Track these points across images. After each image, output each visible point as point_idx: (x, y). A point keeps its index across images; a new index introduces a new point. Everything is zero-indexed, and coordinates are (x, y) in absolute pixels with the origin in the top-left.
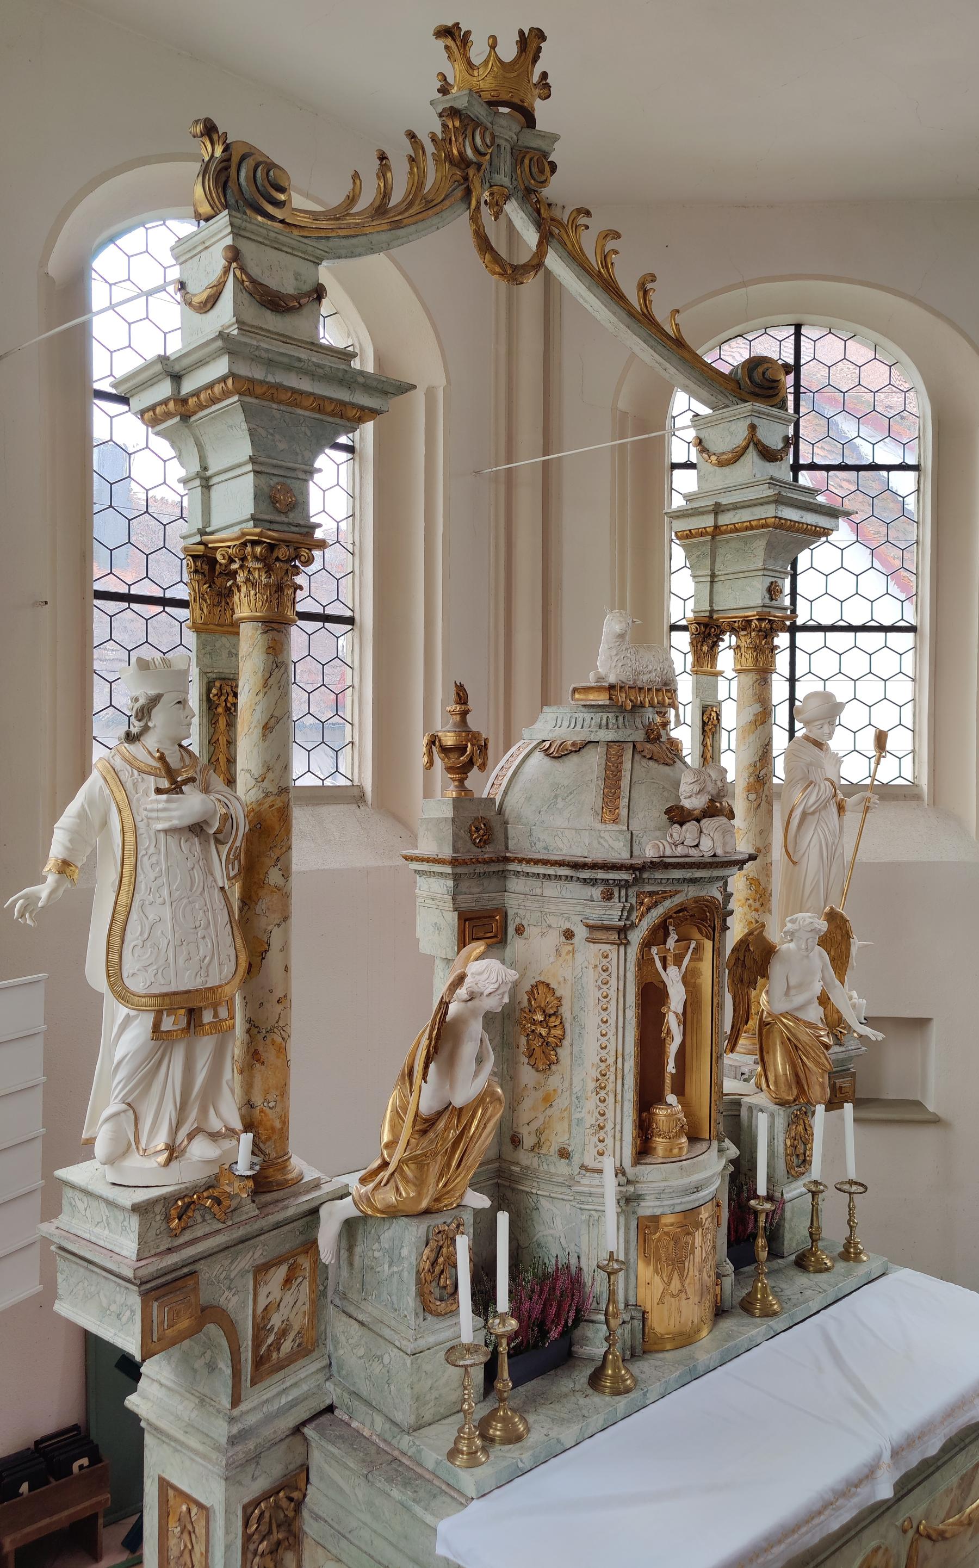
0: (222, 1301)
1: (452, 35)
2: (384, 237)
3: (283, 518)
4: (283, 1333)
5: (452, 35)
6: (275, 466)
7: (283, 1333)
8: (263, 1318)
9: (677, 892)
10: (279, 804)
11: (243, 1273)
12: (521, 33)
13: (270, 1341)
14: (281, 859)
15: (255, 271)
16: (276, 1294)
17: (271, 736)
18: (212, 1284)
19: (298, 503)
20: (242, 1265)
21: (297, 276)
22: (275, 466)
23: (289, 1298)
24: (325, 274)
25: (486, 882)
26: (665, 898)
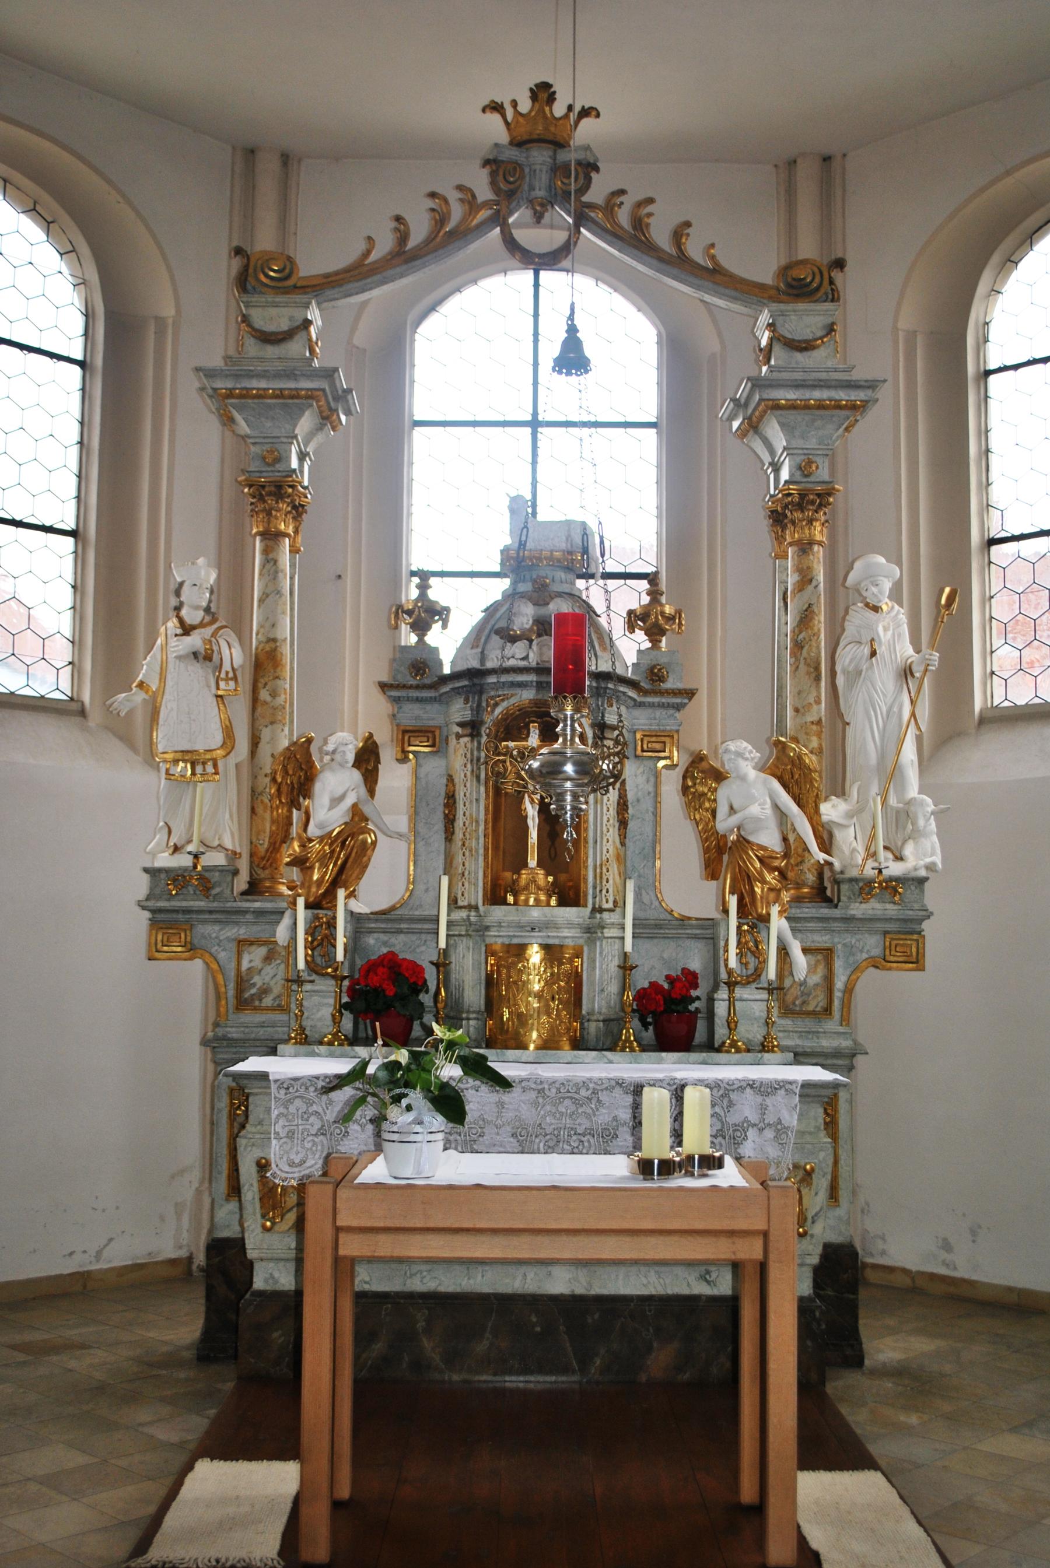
0: (213, 950)
1: (496, 107)
2: (398, 270)
3: (272, 469)
4: (265, 991)
5: (496, 107)
6: (264, 438)
7: (265, 991)
8: (247, 974)
9: (512, 695)
10: (268, 649)
11: (228, 939)
12: (531, 90)
13: (253, 991)
14: (269, 684)
16: (258, 963)
17: (263, 606)
18: (205, 938)
19: (281, 458)
20: (229, 934)
21: (291, 318)
22: (264, 438)
23: (269, 970)
24: (314, 314)
25: (428, 707)
26: (503, 700)
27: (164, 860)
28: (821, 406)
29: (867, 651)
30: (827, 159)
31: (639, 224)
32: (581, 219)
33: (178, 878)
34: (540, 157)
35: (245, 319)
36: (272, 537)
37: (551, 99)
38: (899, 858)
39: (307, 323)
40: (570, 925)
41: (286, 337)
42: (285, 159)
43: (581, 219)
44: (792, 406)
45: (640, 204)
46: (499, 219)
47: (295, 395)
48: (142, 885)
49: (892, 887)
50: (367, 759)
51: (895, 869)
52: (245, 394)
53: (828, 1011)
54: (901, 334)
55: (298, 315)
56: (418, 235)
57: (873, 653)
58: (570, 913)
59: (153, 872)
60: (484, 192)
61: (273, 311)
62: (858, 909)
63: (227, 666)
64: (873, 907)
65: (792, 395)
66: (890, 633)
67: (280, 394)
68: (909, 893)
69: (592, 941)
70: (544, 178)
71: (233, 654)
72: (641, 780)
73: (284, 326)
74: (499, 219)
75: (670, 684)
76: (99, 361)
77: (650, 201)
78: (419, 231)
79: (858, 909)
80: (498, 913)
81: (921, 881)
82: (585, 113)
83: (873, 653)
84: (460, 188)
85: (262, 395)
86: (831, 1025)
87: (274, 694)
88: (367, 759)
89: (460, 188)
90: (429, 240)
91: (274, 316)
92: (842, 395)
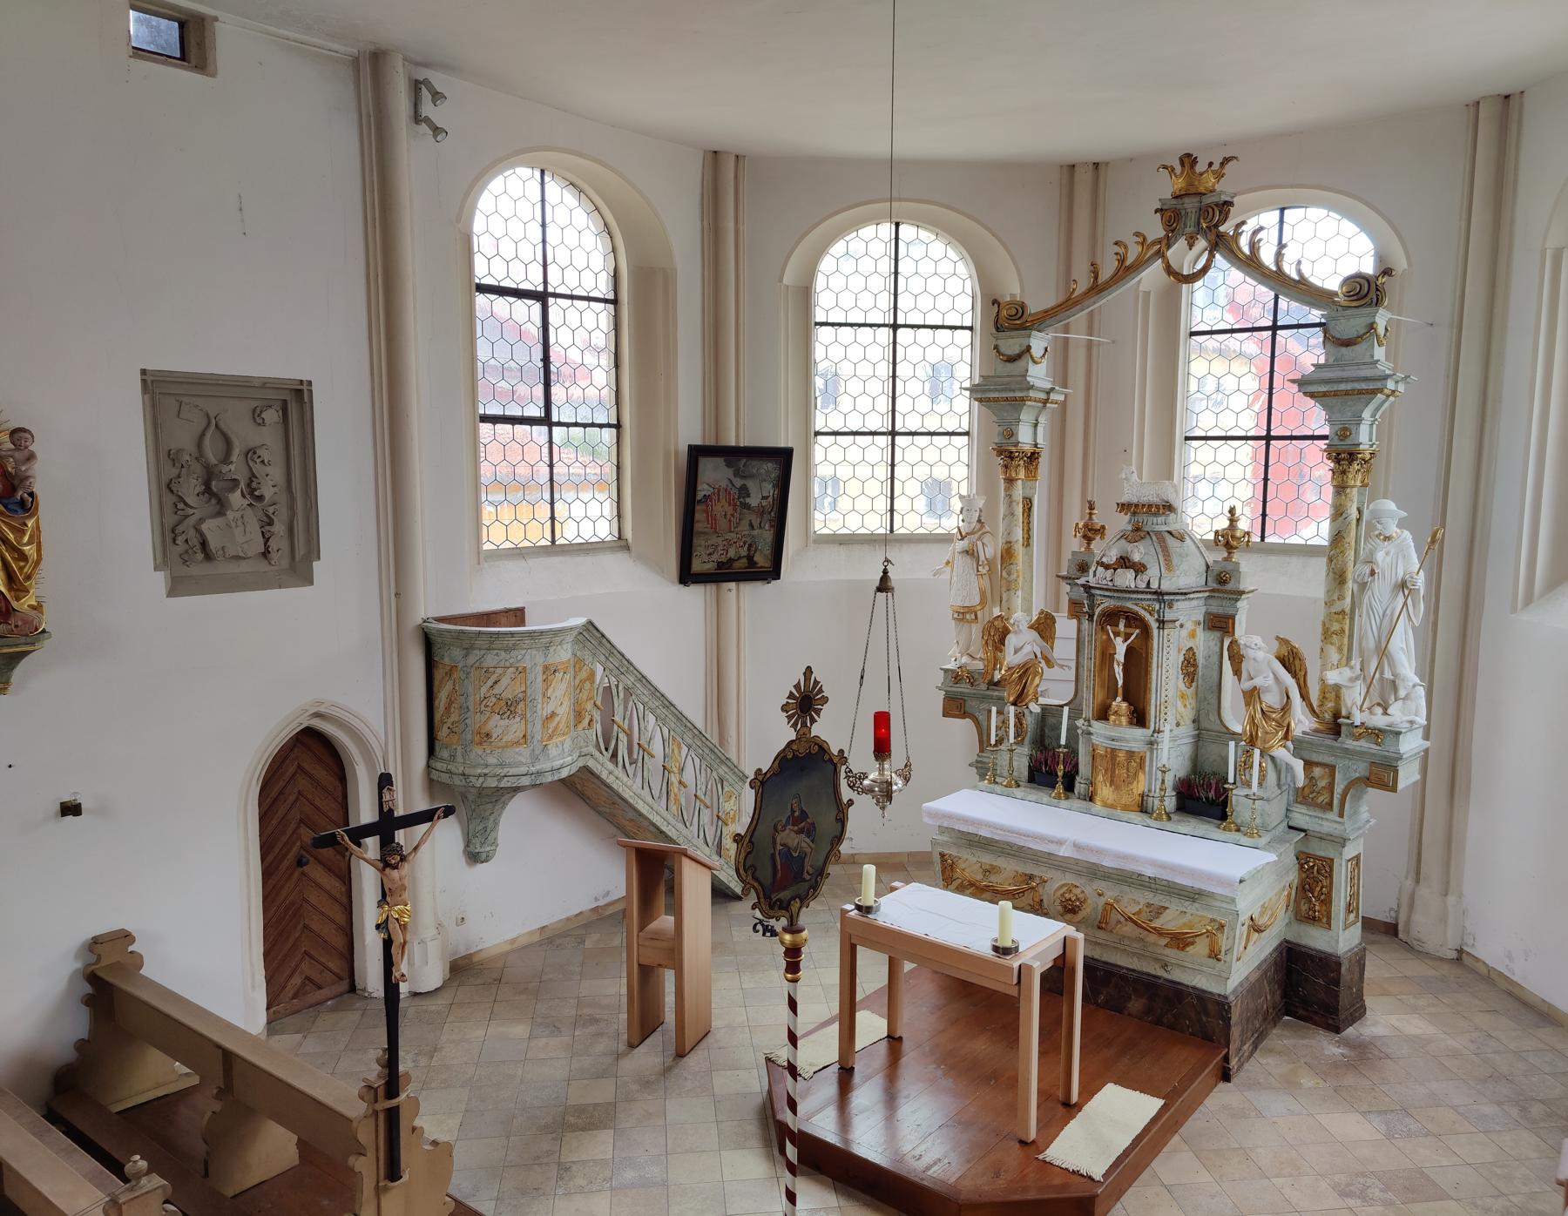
15: (1003, 350)
27: (951, 666)
28: (1347, 393)
29: (1367, 570)
30: (1507, 97)
31: (1254, 246)
32: (1213, 248)
33: (955, 676)
34: (1190, 204)
35: (996, 347)
36: (1010, 481)
37: (1195, 161)
38: (1385, 713)
39: (1029, 348)
40: (1135, 740)
41: (1018, 357)
42: (1096, 165)
43: (1213, 248)
44: (1325, 394)
45: (1255, 232)
46: (1160, 254)
47: (1015, 399)
48: (940, 678)
49: (1376, 734)
50: (1044, 626)
51: (1378, 720)
52: (989, 400)
53: (1330, 804)
54: (1549, 254)
55: (1024, 342)
56: (1106, 272)
57: (1373, 573)
58: (1139, 732)
59: (946, 671)
60: (1156, 230)
61: (1011, 341)
62: (1350, 744)
63: (982, 558)
64: (1363, 744)
65: (1323, 389)
66: (1389, 559)
67: (1007, 399)
68: (1389, 740)
69: (1152, 751)
70: (1193, 218)
71: (990, 549)
72: (1212, 644)
73: (1016, 350)
74: (1160, 254)
75: (1229, 587)
76: (978, 327)
77: (1261, 229)
78: (1108, 269)
79: (1350, 744)
80: (1098, 727)
81: (1399, 733)
82: (1226, 161)
83: (1373, 573)
84: (1137, 234)
85: (996, 400)
86: (1333, 815)
87: (1009, 574)
88: (1044, 626)
89: (1137, 234)
90: (1090, 290)
91: (1011, 345)
92: (1363, 386)
